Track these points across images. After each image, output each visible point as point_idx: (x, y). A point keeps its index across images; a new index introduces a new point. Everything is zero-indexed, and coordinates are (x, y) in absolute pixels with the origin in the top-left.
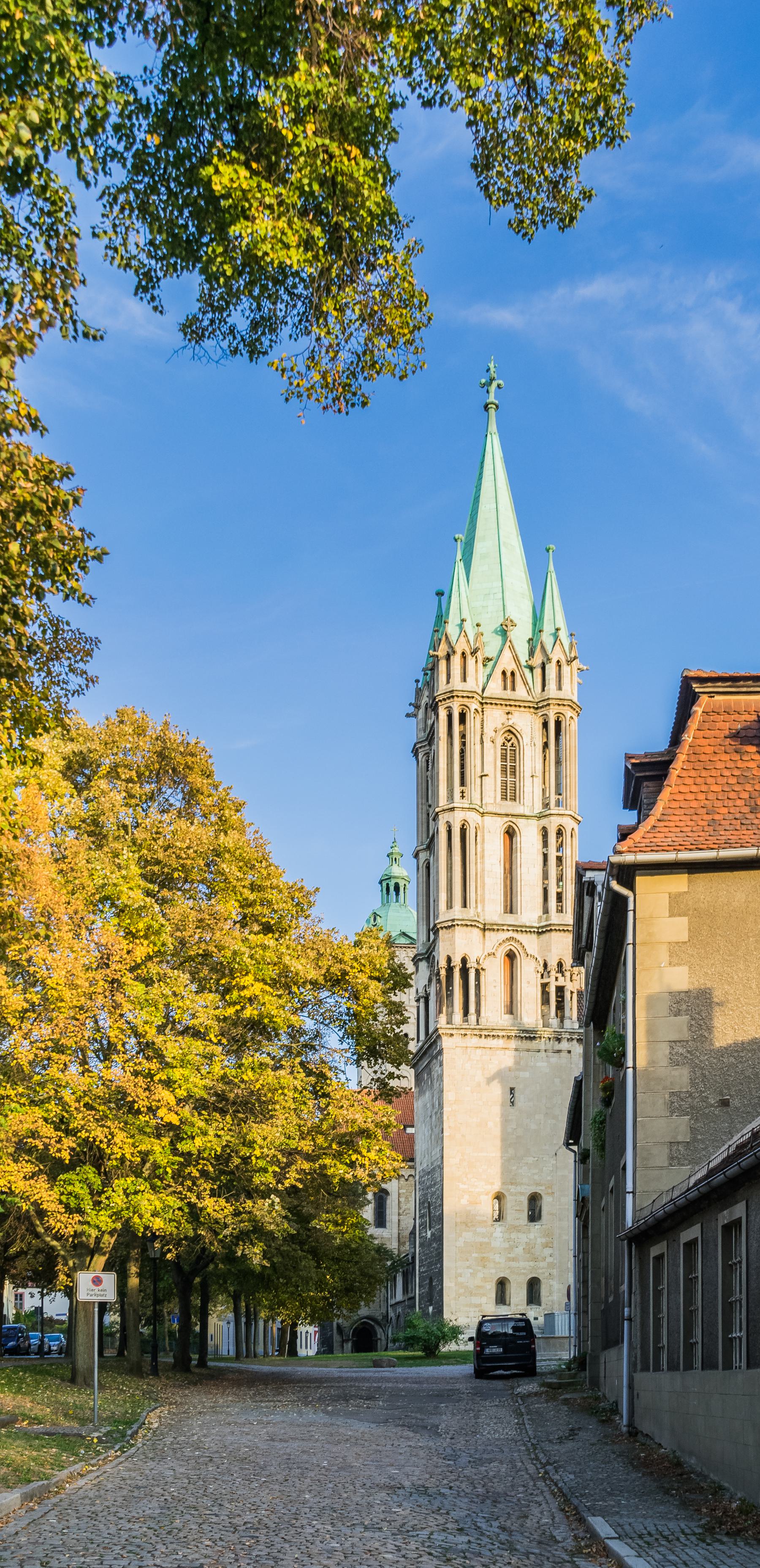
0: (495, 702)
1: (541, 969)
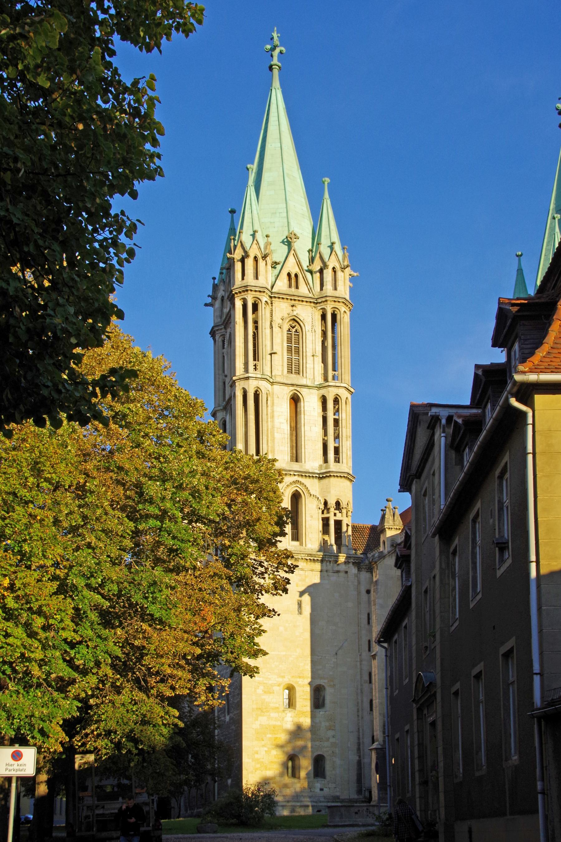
0: (281, 296)
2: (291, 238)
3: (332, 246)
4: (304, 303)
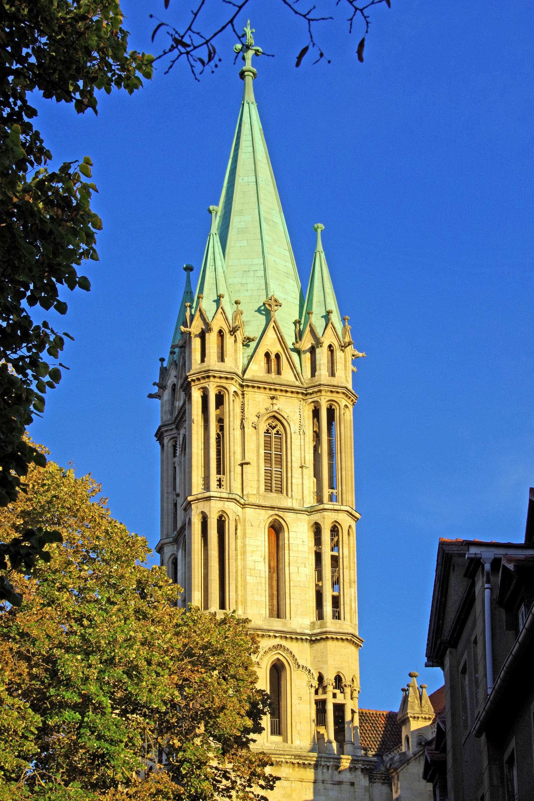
1: (315, 683)
2: (270, 305)
3: (327, 317)
4: (289, 394)
